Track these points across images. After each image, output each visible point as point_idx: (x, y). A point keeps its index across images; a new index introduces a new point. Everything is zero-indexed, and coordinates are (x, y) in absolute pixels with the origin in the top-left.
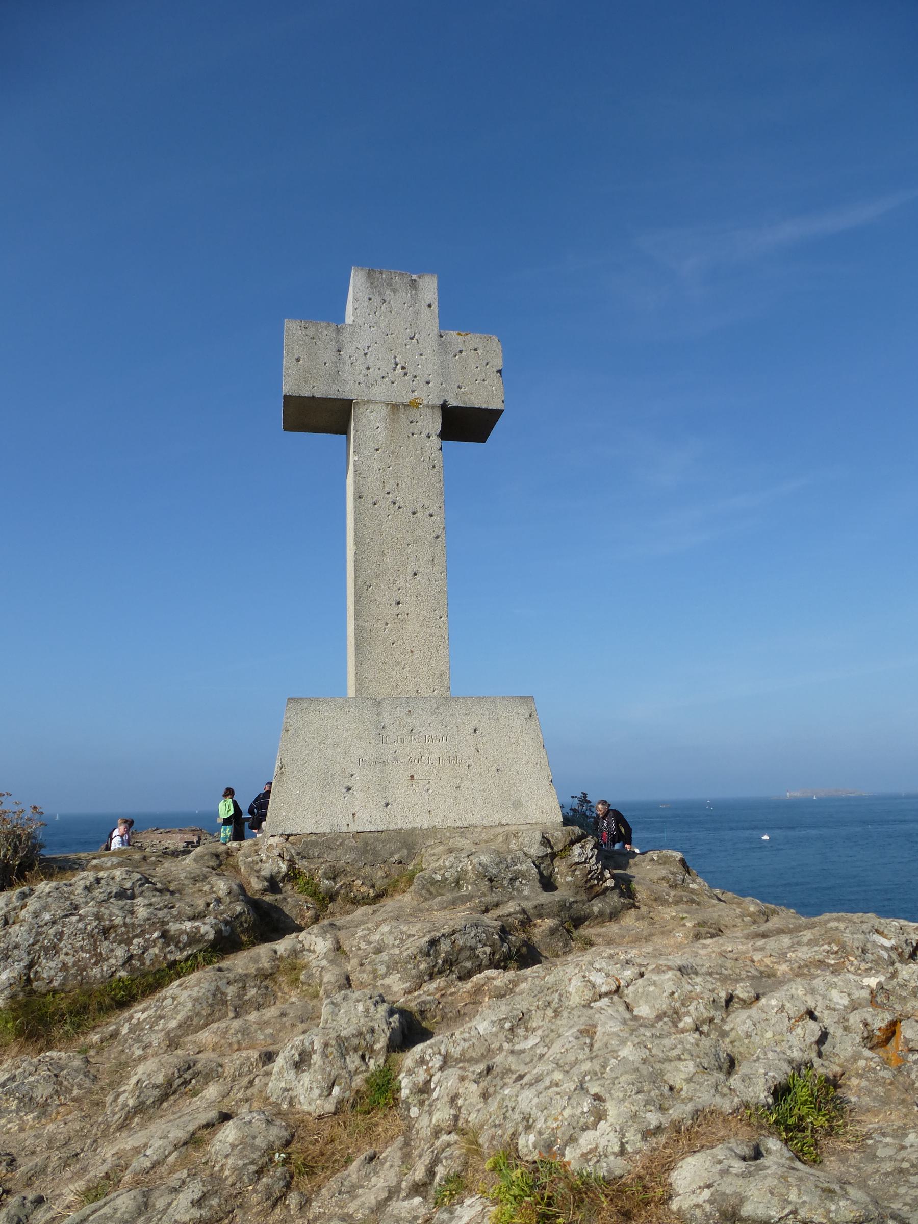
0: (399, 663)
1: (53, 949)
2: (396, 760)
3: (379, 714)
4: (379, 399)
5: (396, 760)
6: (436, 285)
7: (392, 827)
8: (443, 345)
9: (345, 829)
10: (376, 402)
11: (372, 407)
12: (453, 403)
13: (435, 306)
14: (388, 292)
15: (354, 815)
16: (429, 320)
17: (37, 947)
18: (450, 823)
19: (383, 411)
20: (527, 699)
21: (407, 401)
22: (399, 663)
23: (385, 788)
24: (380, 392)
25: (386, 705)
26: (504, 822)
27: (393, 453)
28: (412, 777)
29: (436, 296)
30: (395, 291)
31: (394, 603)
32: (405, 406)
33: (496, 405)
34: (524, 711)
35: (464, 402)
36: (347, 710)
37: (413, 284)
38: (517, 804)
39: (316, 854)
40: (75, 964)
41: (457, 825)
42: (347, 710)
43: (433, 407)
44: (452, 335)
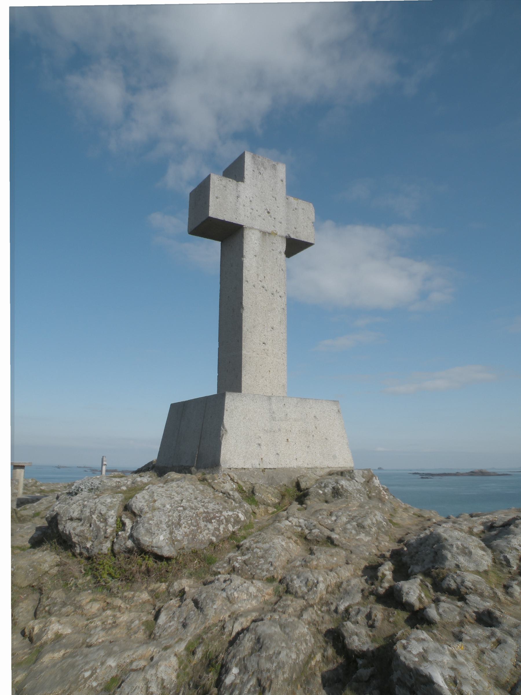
0: (263, 377)
1: (179, 525)
2: (280, 430)
3: (270, 404)
4: (256, 227)
5: (280, 430)
6: (285, 169)
7: (280, 466)
8: (288, 204)
9: (258, 467)
10: (256, 229)
11: (253, 231)
12: (293, 236)
13: (285, 180)
14: (262, 169)
15: (262, 459)
16: (281, 188)
17: (170, 523)
18: (306, 466)
19: (258, 235)
20: (336, 402)
21: (270, 231)
22: (263, 377)
23: (275, 445)
24: (258, 224)
25: (273, 399)
26: (329, 466)
27: (263, 259)
28: (287, 440)
29: (285, 176)
30: (265, 169)
31: (261, 343)
32: (269, 234)
33: (313, 242)
34: (335, 408)
35: (297, 237)
36: (255, 401)
37: (274, 167)
38: (335, 457)
39: (246, 479)
40: (190, 533)
41: (309, 467)
42: (255, 401)
43: (282, 237)
44: (292, 199)
